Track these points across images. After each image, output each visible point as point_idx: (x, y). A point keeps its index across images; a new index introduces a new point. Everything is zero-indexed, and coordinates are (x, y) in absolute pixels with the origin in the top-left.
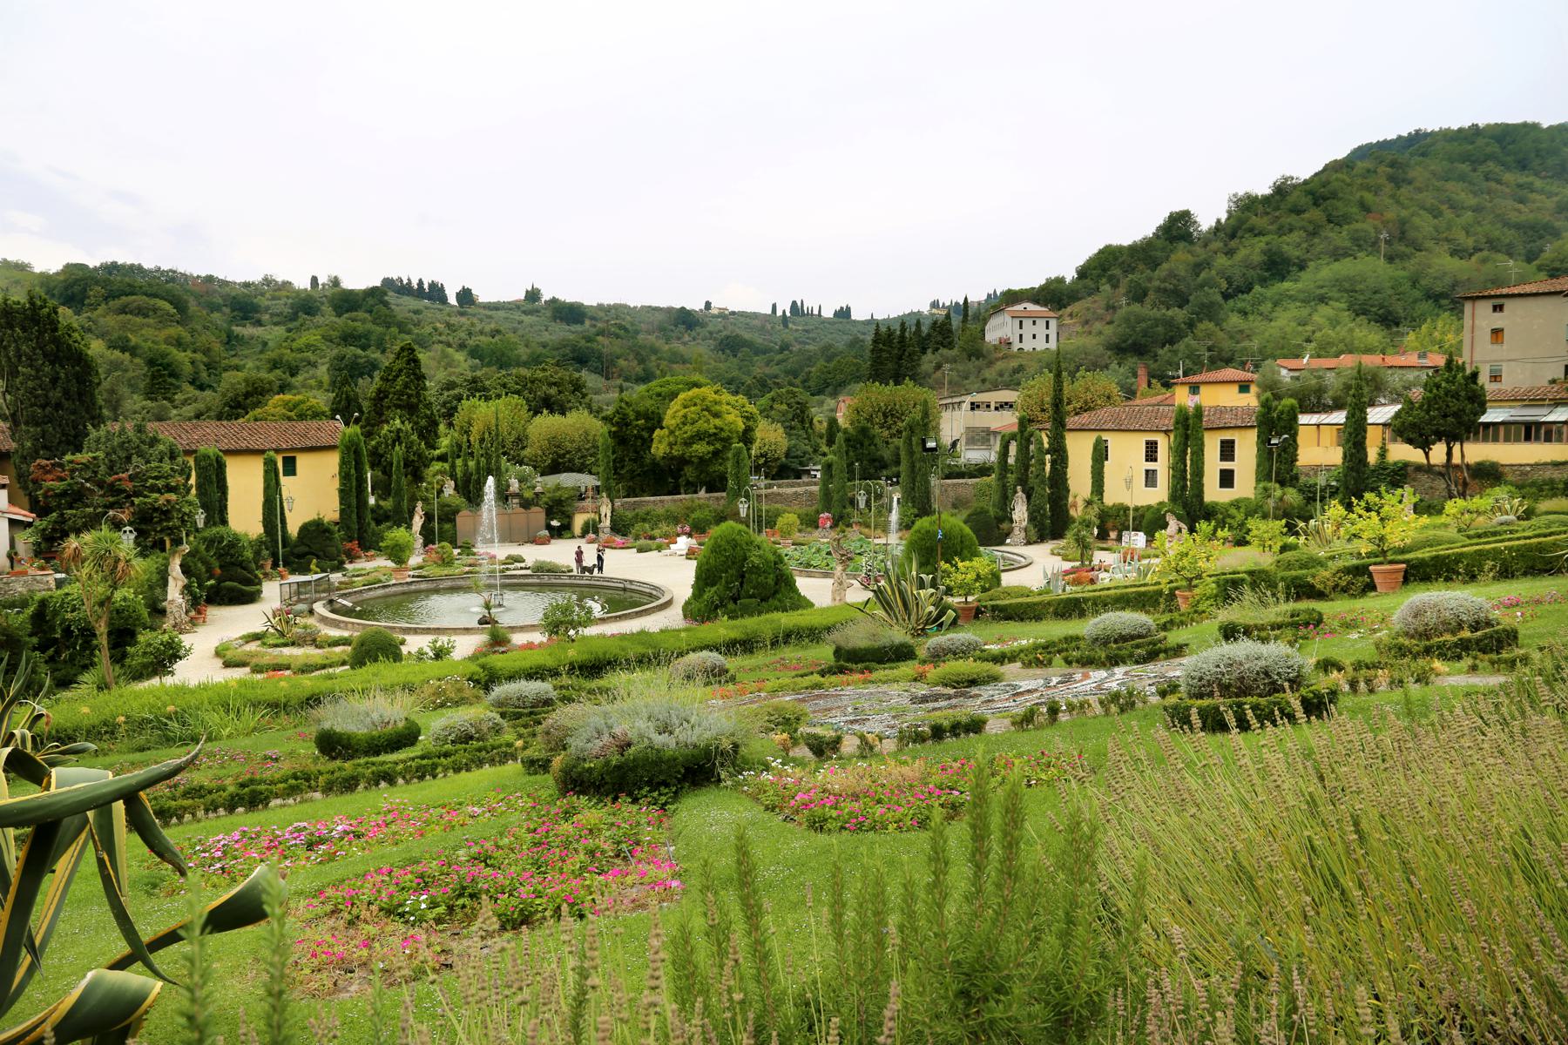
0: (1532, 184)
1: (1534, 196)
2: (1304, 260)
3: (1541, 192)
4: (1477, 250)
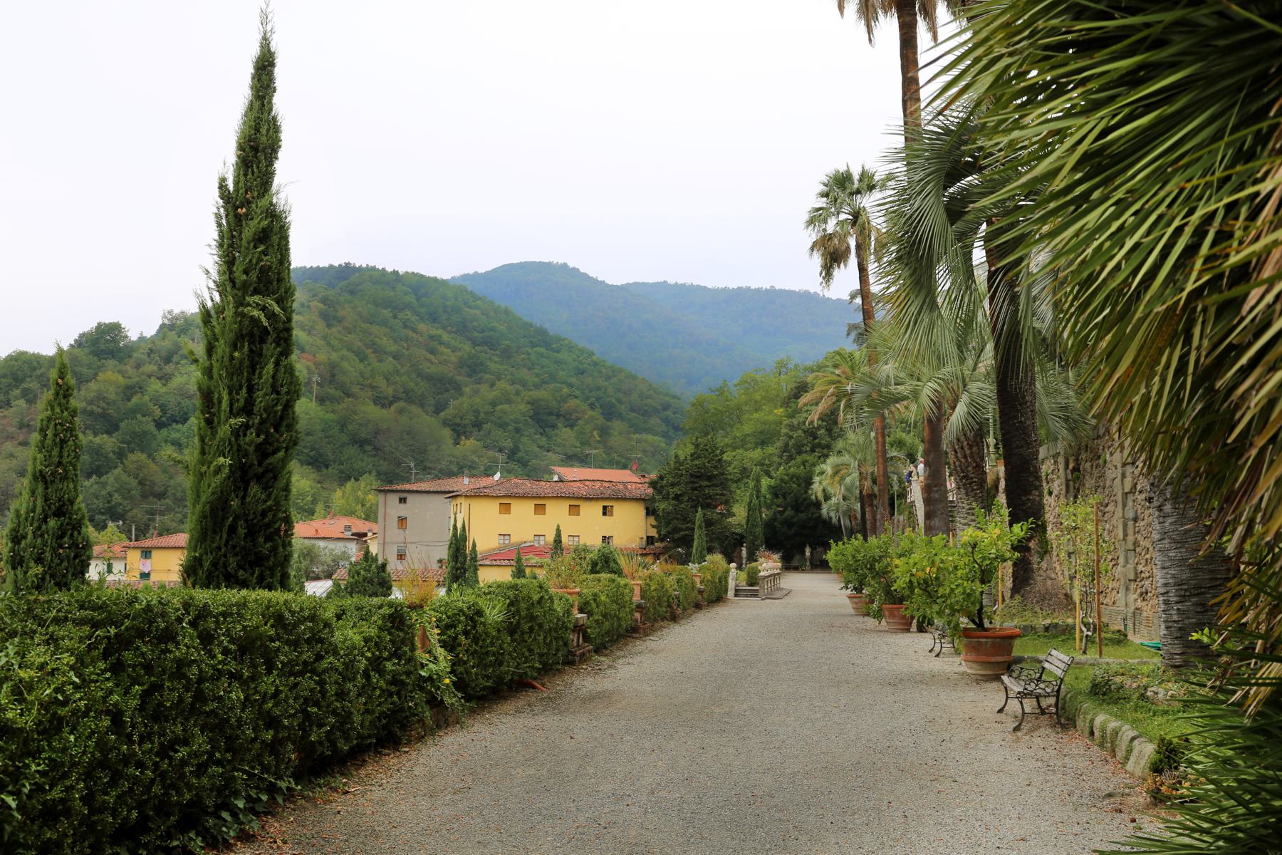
0: (440, 336)
1: (442, 349)
3: (447, 346)
4: (396, 399)
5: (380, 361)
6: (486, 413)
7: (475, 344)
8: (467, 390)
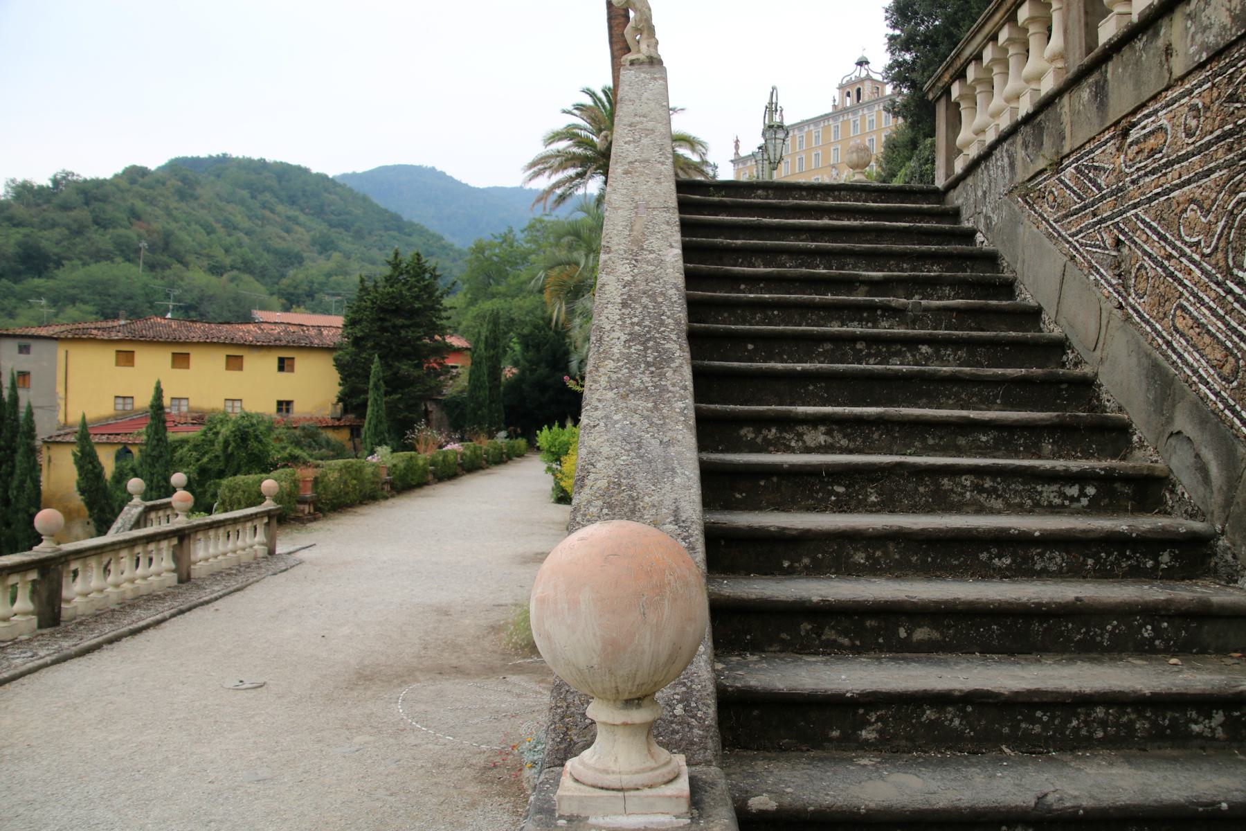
1: (296, 228)
2: (64, 258)
4: (233, 268)
5: (229, 236)
6: (320, 284)
7: (331, 225)
8: (308, 263)
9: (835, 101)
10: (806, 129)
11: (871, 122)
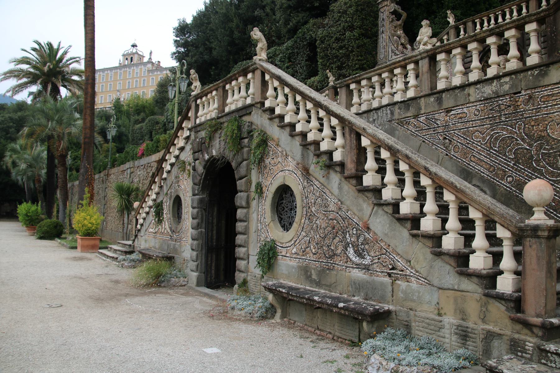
9: (120, 61)
10: (106, 72)
11: (137, 73)
